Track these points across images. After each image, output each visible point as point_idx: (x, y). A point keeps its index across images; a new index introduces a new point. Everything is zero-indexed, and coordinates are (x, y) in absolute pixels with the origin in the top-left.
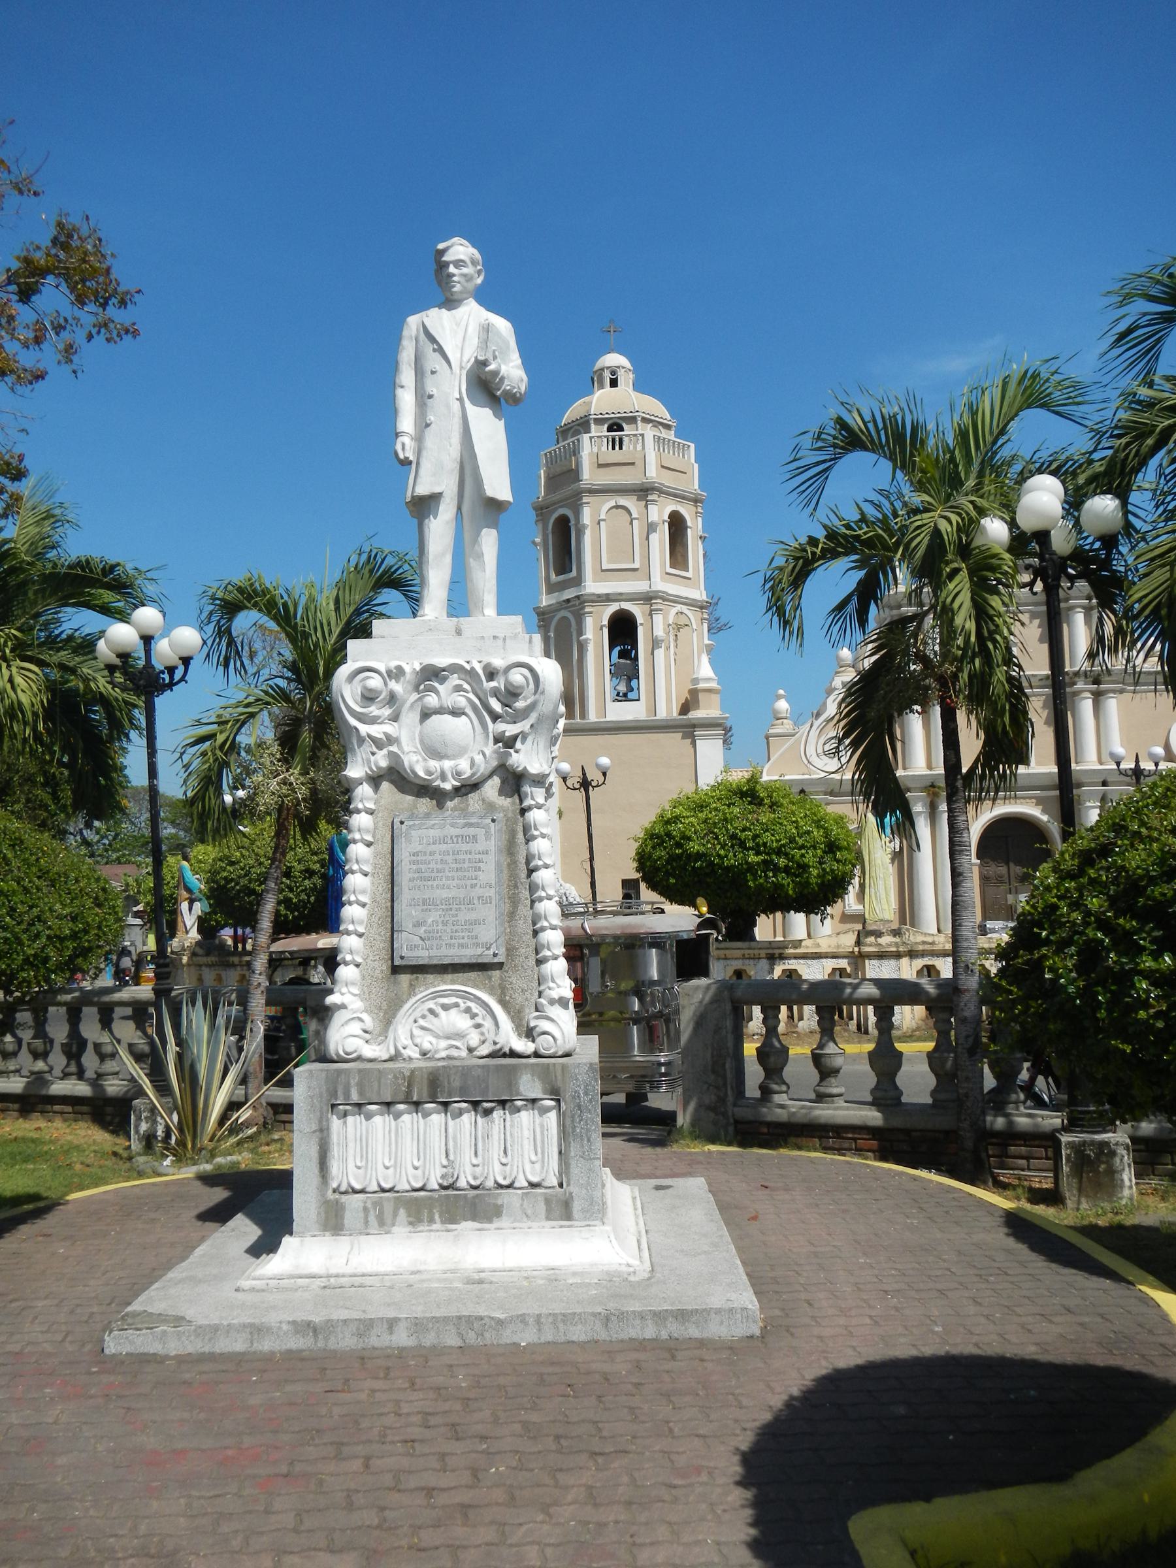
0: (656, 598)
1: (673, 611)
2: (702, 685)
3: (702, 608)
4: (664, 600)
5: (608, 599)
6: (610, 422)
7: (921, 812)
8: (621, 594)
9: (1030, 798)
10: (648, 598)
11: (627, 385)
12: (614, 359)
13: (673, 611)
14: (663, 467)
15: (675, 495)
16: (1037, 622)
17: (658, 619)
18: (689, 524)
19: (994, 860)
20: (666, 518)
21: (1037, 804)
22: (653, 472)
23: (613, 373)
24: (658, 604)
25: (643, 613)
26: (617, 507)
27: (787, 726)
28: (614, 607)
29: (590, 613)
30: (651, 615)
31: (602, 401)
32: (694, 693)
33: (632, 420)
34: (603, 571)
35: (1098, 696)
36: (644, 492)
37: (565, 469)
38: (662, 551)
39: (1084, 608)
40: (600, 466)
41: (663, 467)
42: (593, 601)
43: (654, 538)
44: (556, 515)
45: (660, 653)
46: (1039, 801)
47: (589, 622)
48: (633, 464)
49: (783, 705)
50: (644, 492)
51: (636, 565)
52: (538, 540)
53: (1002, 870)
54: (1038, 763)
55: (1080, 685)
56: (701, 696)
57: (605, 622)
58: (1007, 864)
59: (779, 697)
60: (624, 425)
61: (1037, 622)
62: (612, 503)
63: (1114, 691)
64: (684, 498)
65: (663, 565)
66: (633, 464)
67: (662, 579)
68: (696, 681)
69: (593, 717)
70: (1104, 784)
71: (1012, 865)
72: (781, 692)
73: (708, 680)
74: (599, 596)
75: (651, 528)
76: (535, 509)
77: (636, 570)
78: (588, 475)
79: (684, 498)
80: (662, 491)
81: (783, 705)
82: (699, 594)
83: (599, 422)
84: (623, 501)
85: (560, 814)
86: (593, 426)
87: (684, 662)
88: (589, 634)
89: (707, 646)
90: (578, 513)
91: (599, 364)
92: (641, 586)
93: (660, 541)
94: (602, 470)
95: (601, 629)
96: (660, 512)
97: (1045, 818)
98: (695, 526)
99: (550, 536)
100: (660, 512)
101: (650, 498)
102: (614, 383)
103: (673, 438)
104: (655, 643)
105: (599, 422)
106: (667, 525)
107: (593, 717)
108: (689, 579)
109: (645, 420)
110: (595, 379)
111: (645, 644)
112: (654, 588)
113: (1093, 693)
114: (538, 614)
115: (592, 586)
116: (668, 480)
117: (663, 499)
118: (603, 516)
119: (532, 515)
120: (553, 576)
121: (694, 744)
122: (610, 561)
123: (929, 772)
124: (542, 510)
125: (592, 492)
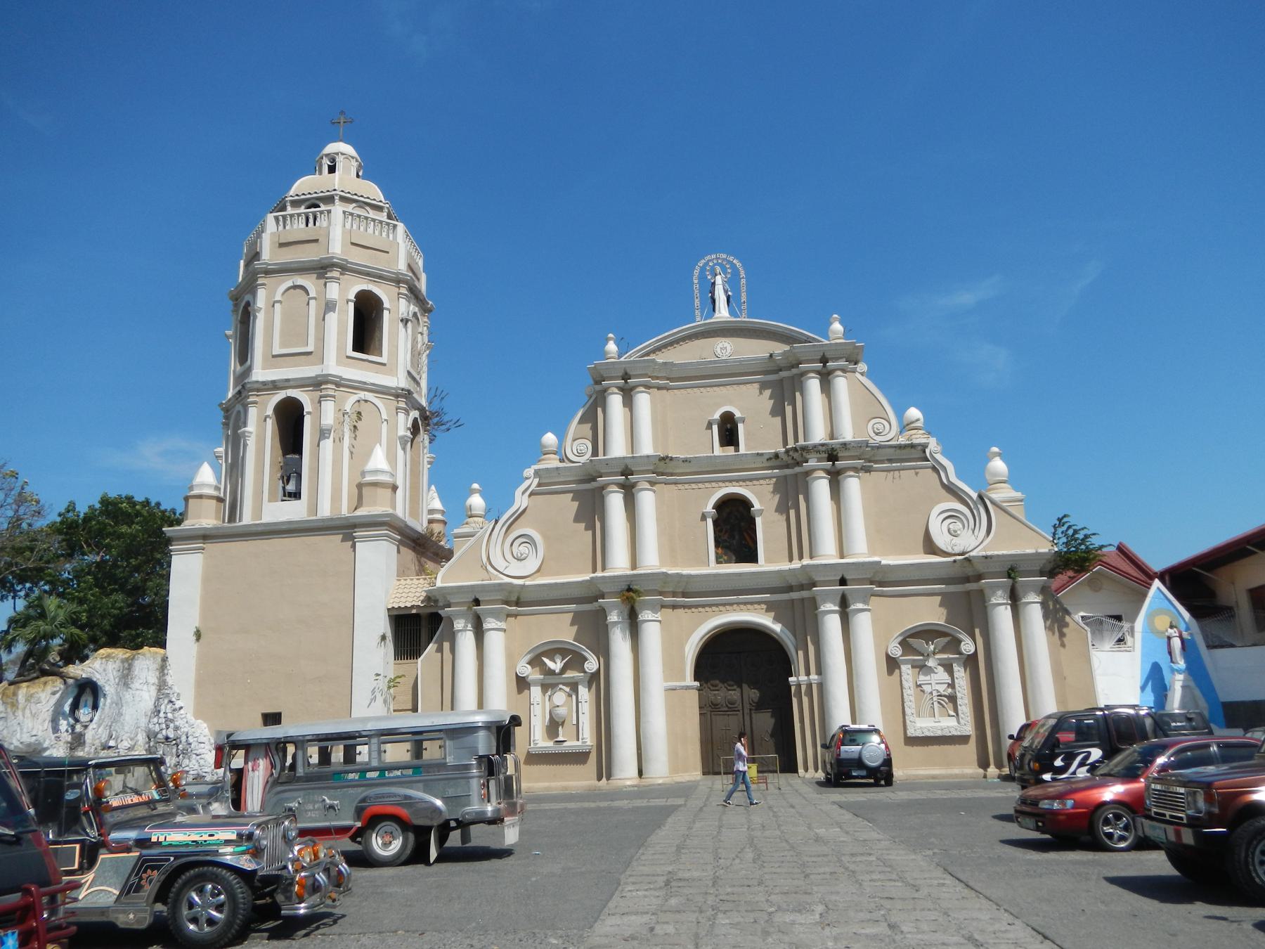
0: (327, 382)
1: (354, 398)
2: (369, 478)
3: (397, 396)
4: (338, 385)
5: (274, 386)
6: (308, 203)
7: (615, 623)
8: (287, 380)
9: (759, 603)
10: (317, 384)
11: (347, 170)
12: (331, 148)
13: (354, 398)
14: (352, 244)
15: (368, 274)
16: (768, 393)
17: (329, 407)
18: (386, 304)
19: (723, 681)
20: (352, 296)
21: (767, 610)
22: (337, 248)
23: (333, 160)
24: (330, 389)
25: (311, 400)
26: (295, 287)
27: (474, 525)
28: (281, 395)
29: (255, 403)
30: (320, 402)
31: (304, 185)
32: (360, 486)
33: (329, 200)
34: (274, 356)
35: (835, 478)
36: (322, 269)
37: (253, 253)
38: (341, 333)
39: (818, 373)
40: (282, 245)
41: (352, 244)
42: (258, 390)
43: (332, 318)
44: (243, 304)
45: (327, 445)
46: (770, 607)
47: (253, 412)
48: (316, 241)
49: (477, 501)
50: (322, 269)
51: (310, 348)
52: (229, 333)
53: (734, 694)
54: (768, 560)
55: (812, 463)
56: (365, 491)
57: (270, 411)
58: (741, 687)
59: (473, 492)
60: (321, 205)
61: (768, 393)
62: (290, 284)
63: (855, 469)
64: (381, 277)
65: (341, 348)
66: (316, 241)
67: (339, 363)
68: (363, 474)
69: (247, 518)
70: (843, 582)
71: (745, 686)
72: (476, 486)
73: (376, 472)
74: (264, 383)
75: (330, 306)
76: (231, 298)
77: (309, 353)
78: (268, 254)
79: (381, 277)
80: (345, 268)
81: (477, 501)
82: (399, 381)
83: (296, 204)
84: (300, 280)
85: (198, 635)
86: (289, 208)
87: (360, 455)
88: (251, 427)
89: (401, 438)
90: (254, 294)
91: (321, 154)
92: (309, 371)
93: (342, 324)
94: (285, 249)
95: (265, 420)
96: (344, 291)
97: (777, 628)
98: (395, 305)
99: (239, 326)
100: (343, 291)
101: (329, 275)
102: (332, 169)
103: (385, 219)
104: (323, 434)
105: (296, 204)
106: (351, 306)
107: (247, 518)
108: (384, 365)
109: (343, 199)
110: (314, 169)
111: (312, 434)
112: (324, 372)
113: (828, 472)
114: (223, 409)
115: (260, 374)
116: (358, 257)
117: (347, 277)
118: (278, 297)
119: (230, 304)
120: (239, 367)
121: (354, 546)
122: (283, 345)
123: (632, 572)
124: (236, 298)
125: (268, 272)
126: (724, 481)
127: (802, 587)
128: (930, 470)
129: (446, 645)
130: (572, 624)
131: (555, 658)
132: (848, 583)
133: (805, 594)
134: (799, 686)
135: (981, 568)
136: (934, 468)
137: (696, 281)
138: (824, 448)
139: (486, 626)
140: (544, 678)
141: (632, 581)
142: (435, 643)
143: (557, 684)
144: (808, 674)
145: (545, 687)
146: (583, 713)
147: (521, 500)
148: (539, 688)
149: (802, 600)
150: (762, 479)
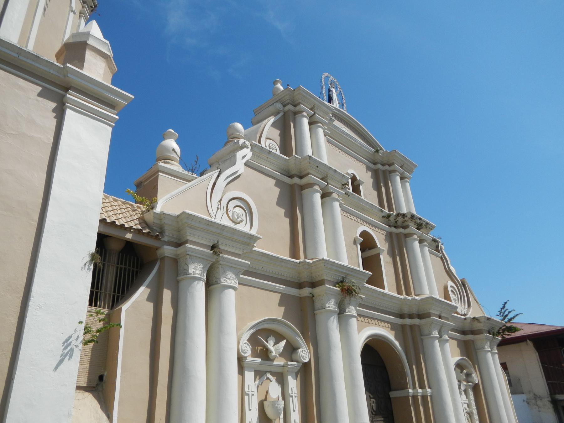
9: (388, 322)
21: (392, 329)
46: (394, 327)
59: (170, 136)
126: (366, 222)
127: (411, 316)
128: (439, 259)
129: (167, 295)
130: (280, 304)
131: (270, 338)
132: (442, 318)
133: (416, 321)
134: (415, 397)
135: (477, 326)
136: (441, 258)
137: (323, 83)
138: (418, 221)
139: (224, 281)
140: (261, 364)
141: (348, 274)
142: (148, 287)
143: (265, 372)
144: (414, 388)
145: (259, 374)
146: (250, 410)
147: (239, 167)
148: (253, 374)
149: (411, 327)
150: (381, 229)
